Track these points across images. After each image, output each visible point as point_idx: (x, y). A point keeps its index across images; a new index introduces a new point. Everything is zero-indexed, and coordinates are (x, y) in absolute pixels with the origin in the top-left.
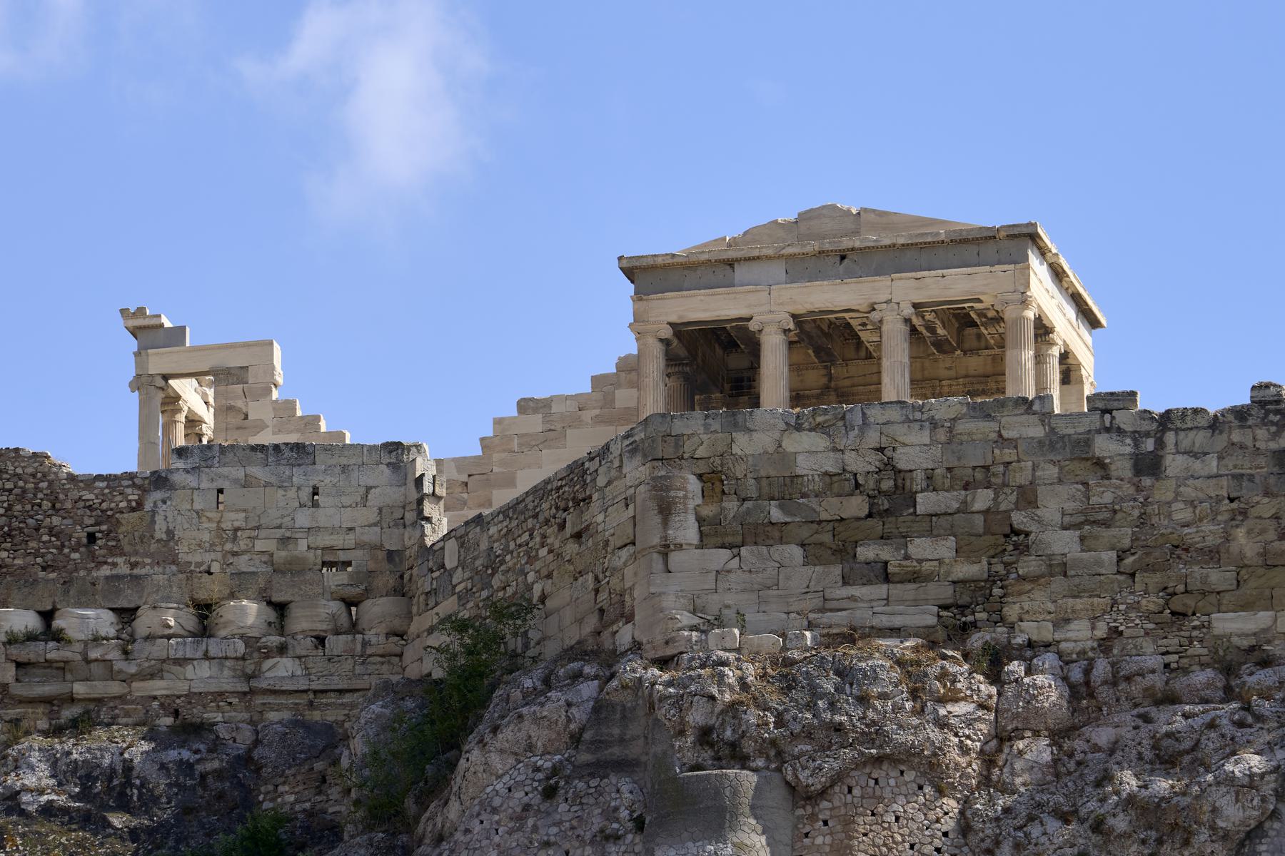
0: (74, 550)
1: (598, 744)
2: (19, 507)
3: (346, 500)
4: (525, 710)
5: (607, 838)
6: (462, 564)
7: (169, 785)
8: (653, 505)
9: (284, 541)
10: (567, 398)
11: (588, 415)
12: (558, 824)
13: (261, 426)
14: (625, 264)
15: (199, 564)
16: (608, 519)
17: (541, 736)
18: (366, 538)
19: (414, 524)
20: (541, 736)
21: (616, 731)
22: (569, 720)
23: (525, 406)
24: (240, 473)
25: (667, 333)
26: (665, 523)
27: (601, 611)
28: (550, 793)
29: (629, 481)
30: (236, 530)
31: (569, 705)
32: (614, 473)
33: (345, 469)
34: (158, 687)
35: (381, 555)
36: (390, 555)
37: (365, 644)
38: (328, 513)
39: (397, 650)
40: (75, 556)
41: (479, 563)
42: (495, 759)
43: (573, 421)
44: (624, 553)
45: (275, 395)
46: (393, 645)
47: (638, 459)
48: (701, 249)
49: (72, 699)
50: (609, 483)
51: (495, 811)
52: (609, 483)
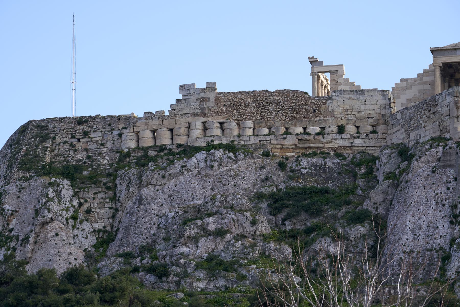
0: (311, 114)
1: (444, 161)
2: (298, 104)
3: (372, 103)
4: (427, 153)
5: (448, 182)
6: (402, 118)
7: (335, 168)
8: (454, 107)
9: (358, 112)
10: (412, 79)
11: (416, 83)
12: (436, 179)
13: (341, 84)
14: (431, 49)
15: (339, 117)
16: (442, 110)
17: (431, 159)
18: (377, 112)
19: (388, 109)
20: (431, 159)
21: (449, 158)
22: (437, 156)
23: (402, 80)
24: (348, 97)
25: (441, 65)
26: (458, 111)
27: (441, 130)
28: (434, 172)
29: (448, 101)
30: (347, 109)
31: (437, 152)
32: (444, 99)
33: (372, 96)
34: (331, 145)
35: (381, 115)
36: (383, 115)
37: (378, 136)
38: (368, 106)
39: (385, 137)
40: (311, 115)
41: (407, 118)
42: (420, 164)
43: (414, 84)
44: (447, 117)
45: (344, 77)
46: (384, 136)
47: (450, 96)
48: (449, 46)
49: (311, 148)
50: (442, 101)
51: (421, 176)
52: (442, 101)
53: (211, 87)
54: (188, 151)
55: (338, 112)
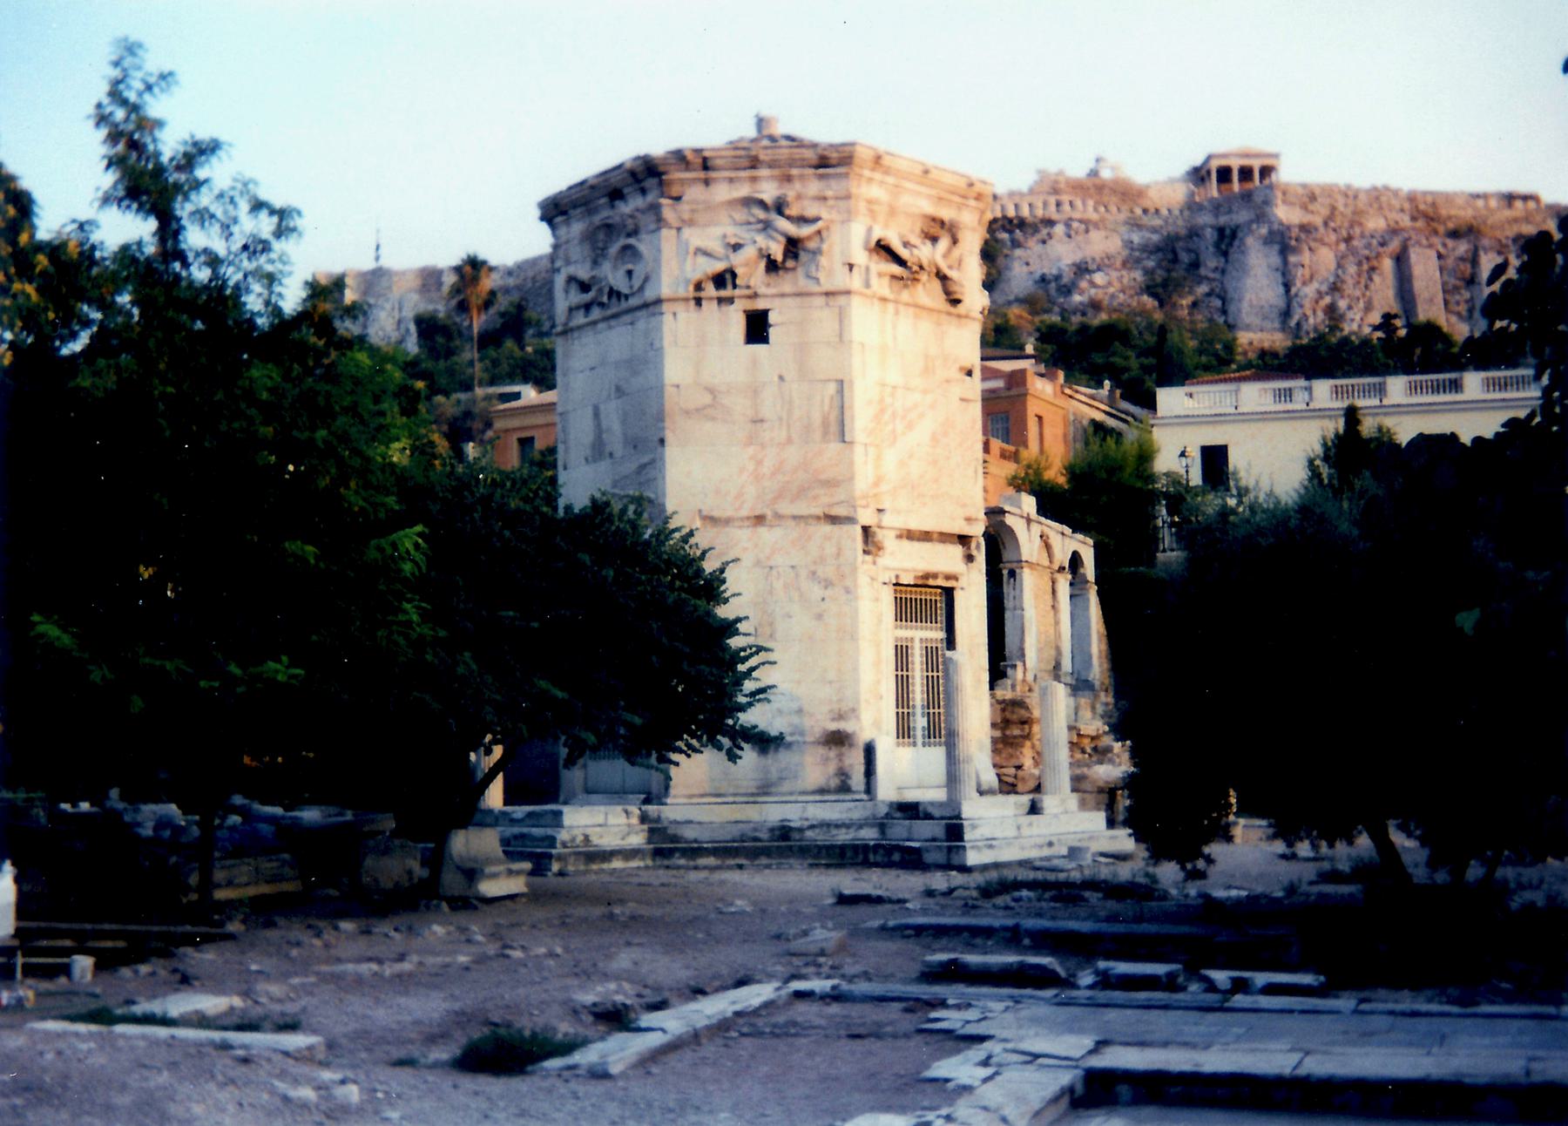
54: (1050, 223)
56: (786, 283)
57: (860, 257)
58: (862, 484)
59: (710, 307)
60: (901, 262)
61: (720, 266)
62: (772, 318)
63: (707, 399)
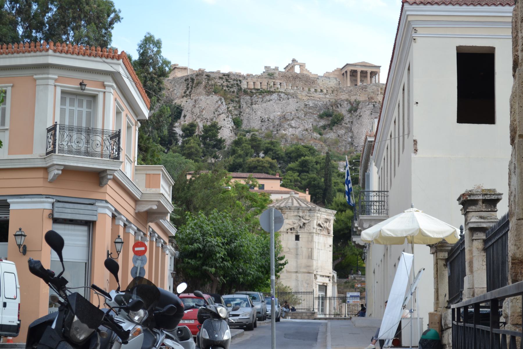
38: (331, 83)
53: (277, 69)
55: (321, 84)
56: (302, 230)
57: (315, 227)
58: (314, 267)
59: (289, 234)
60: (321, 227)
61: (291, 227)
62: (300, 236)
63: (288, 250)
